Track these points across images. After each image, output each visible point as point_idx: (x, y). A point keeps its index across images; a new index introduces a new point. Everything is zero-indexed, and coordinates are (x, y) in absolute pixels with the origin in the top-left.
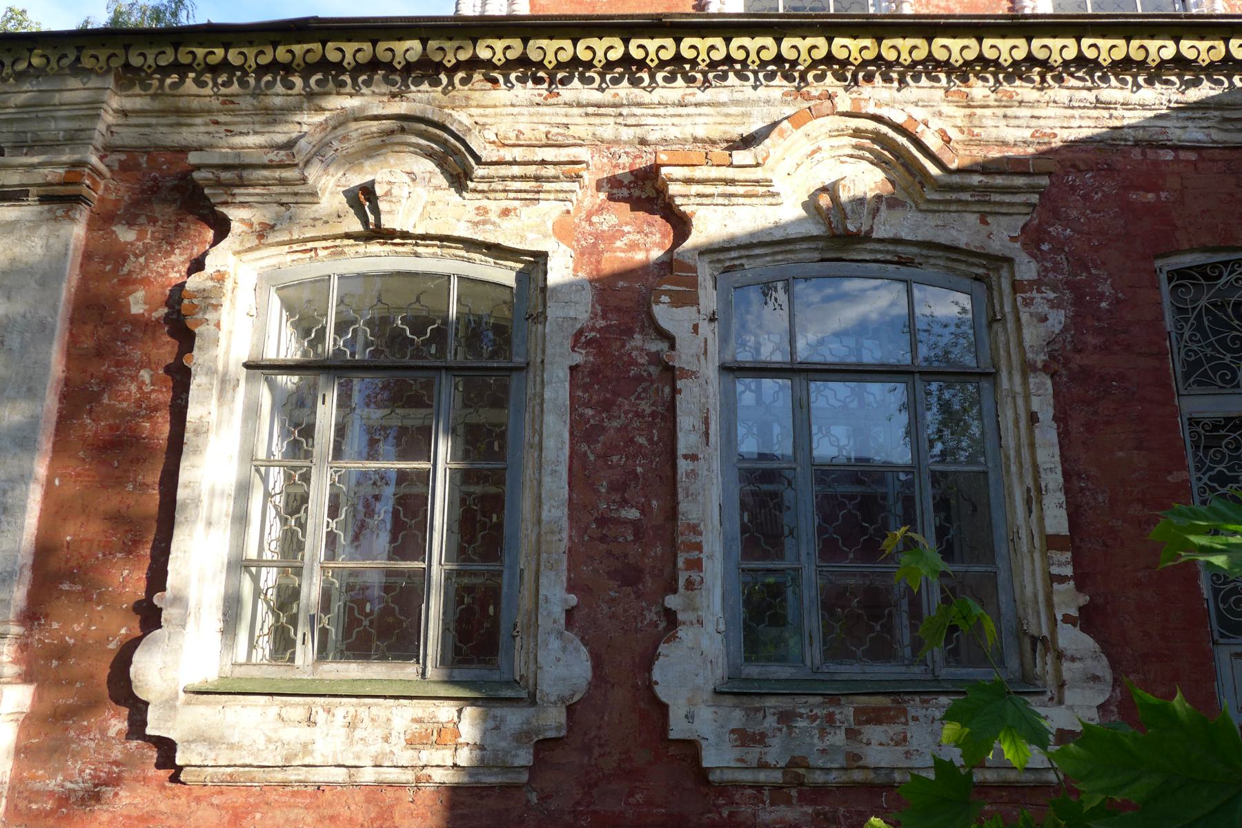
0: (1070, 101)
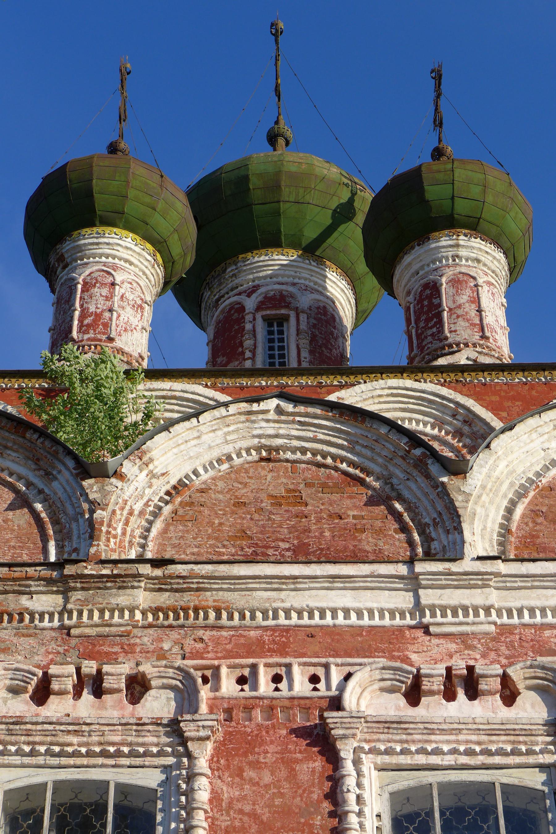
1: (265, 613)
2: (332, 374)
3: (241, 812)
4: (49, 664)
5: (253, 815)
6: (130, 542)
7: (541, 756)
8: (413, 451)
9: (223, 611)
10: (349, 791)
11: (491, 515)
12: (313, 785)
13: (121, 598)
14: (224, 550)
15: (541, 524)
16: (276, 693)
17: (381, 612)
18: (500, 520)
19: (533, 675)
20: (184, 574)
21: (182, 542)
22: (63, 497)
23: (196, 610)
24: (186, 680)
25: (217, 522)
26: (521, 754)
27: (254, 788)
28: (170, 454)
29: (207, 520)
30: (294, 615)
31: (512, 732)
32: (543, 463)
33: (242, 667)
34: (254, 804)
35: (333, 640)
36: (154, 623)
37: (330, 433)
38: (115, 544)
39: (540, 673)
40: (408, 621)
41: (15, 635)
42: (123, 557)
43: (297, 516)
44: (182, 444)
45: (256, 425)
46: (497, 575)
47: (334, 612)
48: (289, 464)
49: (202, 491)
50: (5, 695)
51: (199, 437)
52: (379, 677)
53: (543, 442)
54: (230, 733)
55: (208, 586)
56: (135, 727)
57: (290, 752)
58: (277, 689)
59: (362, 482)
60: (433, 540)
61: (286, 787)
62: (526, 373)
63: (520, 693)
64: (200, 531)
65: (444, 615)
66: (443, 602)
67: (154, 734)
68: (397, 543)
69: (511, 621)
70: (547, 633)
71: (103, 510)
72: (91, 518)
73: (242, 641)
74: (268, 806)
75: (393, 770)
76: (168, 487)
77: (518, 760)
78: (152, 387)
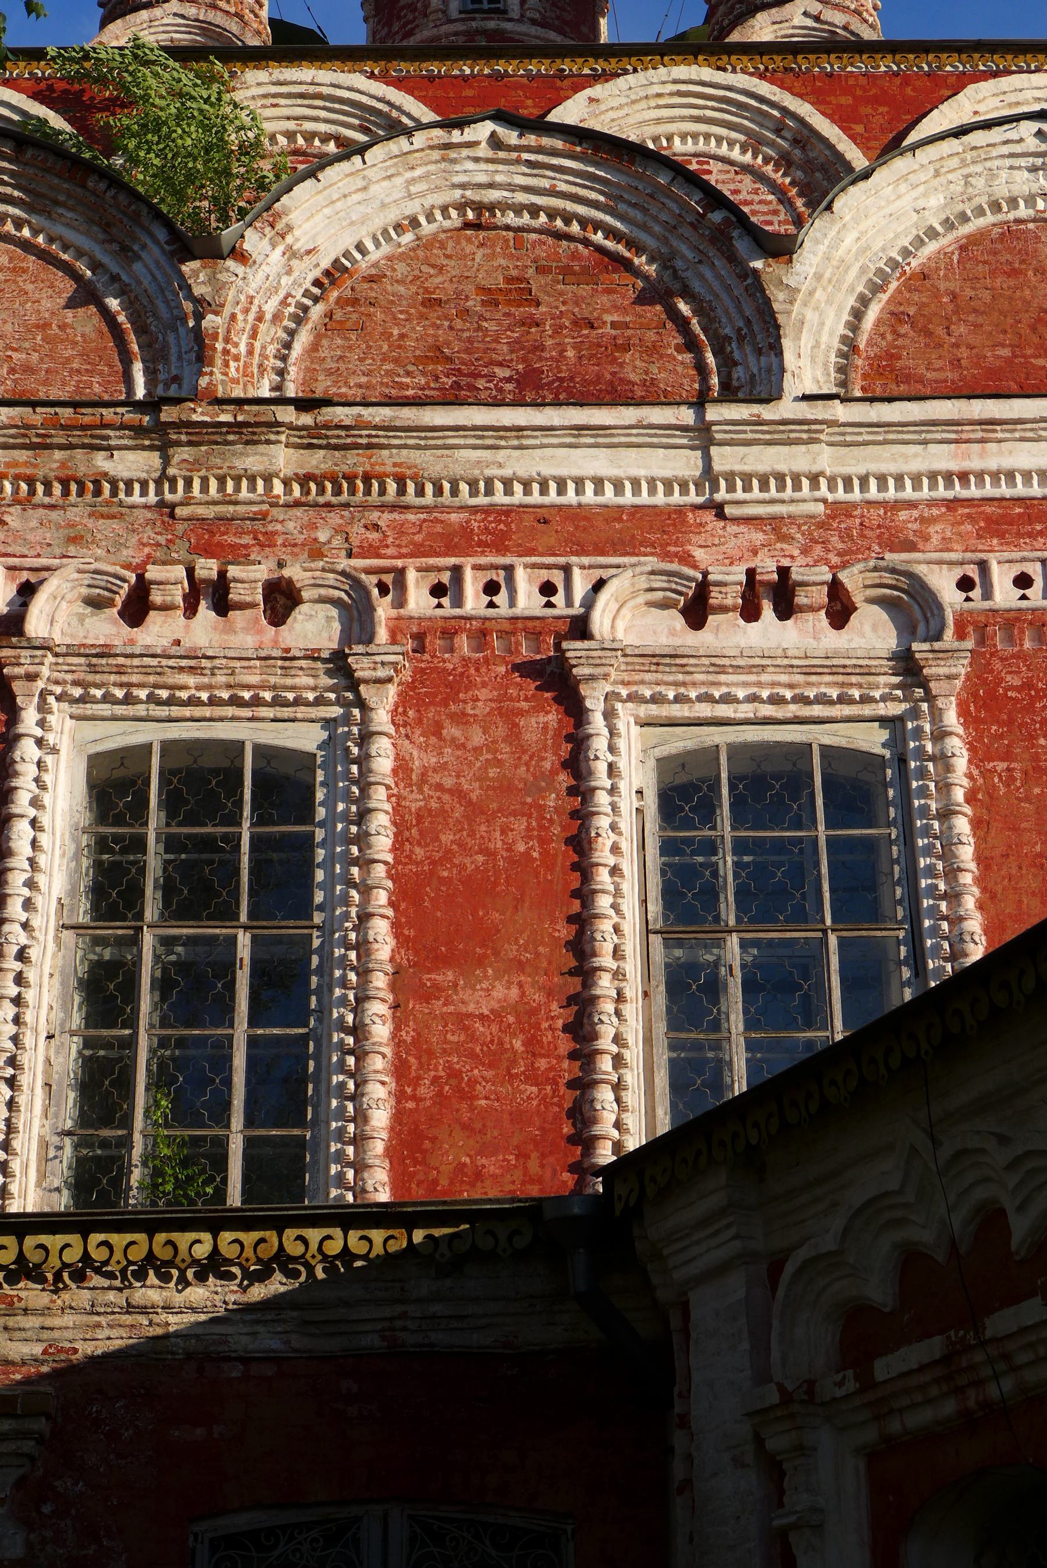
0: (93, 1306)
1: (473, 484)
2: (580, 56)
3: (439, 787)
4: (145, 563)
5: (457, 792)
6: (260, 366)
7: (882, 705)
8: (709, 215)
9: (408, 481)
10: (597, 758)
11: (828, 323)
12: (545, 748)
13: (251, 459)
14: (408, 380)
15: (904, 336)
16: (491, 610)
17: (652, 482)
18: (841, 330)
19: (878, 581)
20: (347, 422)
21: (342, 366)
22: (152, 289)
23: (367, 479)
24: (355, 591)
25: (396, 332)
26: (851, 701)
27: (459, 753)
28: (318, 218)
29: (380, 329)
30: (518, 488)
31: (841, 670)
32: (915, 232)
33: (440, 569)
34: (458, 776)
35: (577, 527)
36: (303, 499)
37: (578, 181)
38: (237, 370)
39: (888, 578)
40: (693, 498)
41: (90, 516)
42: (251, 393)
43: (524, 324)
44: (338, 199)
45: (458, 167)
46: (832, 423)
47: (579, 482)
48: (511, 234)
49: (371, 279)
50: (81, 610)
51: (365, 189)
52: (646, 586)
53: (916, 199)
54: (422, 670)
55: (383, 441)
56: (280, 663)
57: (511, 699)
58: (491, 605)
59: (626, 265)
60: (736, 364)
62: (898, 57)
63: (856, 609)
64: (369, 347)
65: (747, 488)
66: (747, 468)
67: (310, 672)
68: (679, 369)
69: (849, 497)
70: (903, 515)
71: (216, 313)
72: (197, 330)
73: (439, 529)
74: (479, 779)
75: (662, 725)
76: (317, 273)
77: (847, 710)
78: (282, 78)
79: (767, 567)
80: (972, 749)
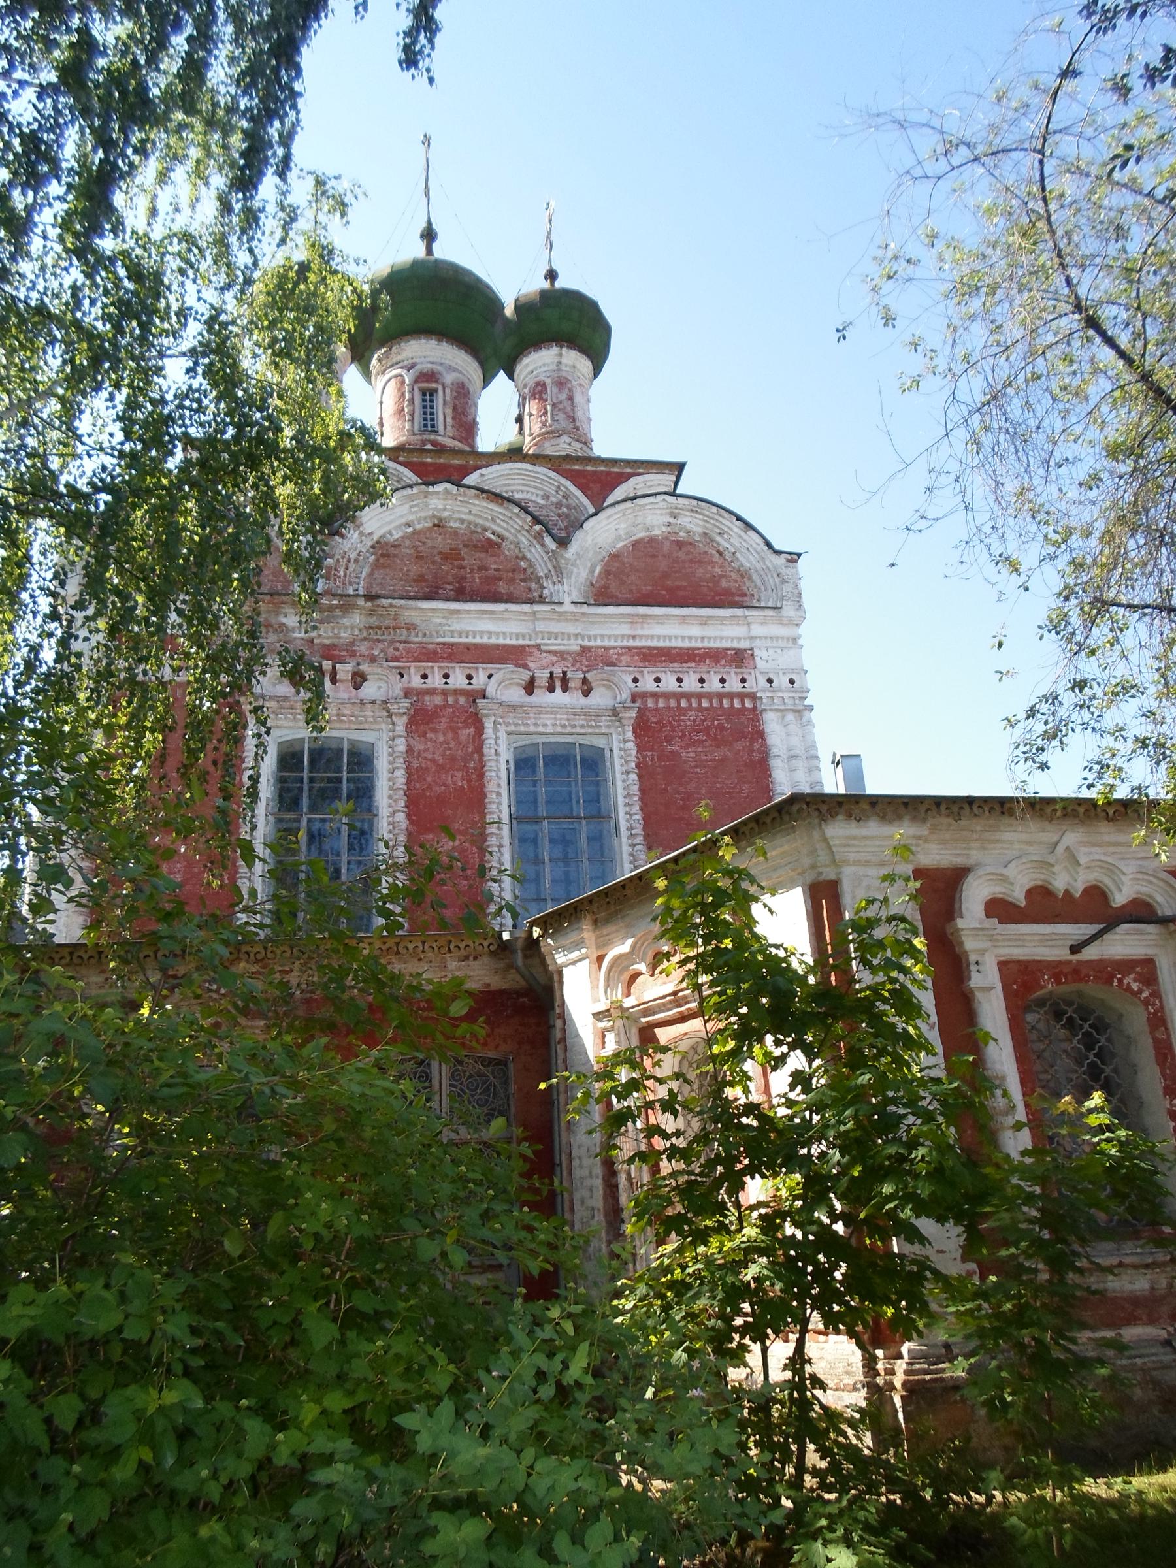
5: (433, 761)
49: (394, 546)
61: (453, 745)
79: (558, 671)
80: (638, 746)
